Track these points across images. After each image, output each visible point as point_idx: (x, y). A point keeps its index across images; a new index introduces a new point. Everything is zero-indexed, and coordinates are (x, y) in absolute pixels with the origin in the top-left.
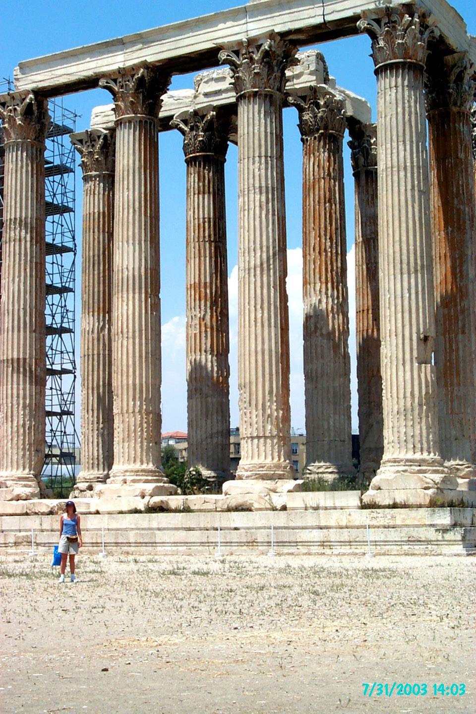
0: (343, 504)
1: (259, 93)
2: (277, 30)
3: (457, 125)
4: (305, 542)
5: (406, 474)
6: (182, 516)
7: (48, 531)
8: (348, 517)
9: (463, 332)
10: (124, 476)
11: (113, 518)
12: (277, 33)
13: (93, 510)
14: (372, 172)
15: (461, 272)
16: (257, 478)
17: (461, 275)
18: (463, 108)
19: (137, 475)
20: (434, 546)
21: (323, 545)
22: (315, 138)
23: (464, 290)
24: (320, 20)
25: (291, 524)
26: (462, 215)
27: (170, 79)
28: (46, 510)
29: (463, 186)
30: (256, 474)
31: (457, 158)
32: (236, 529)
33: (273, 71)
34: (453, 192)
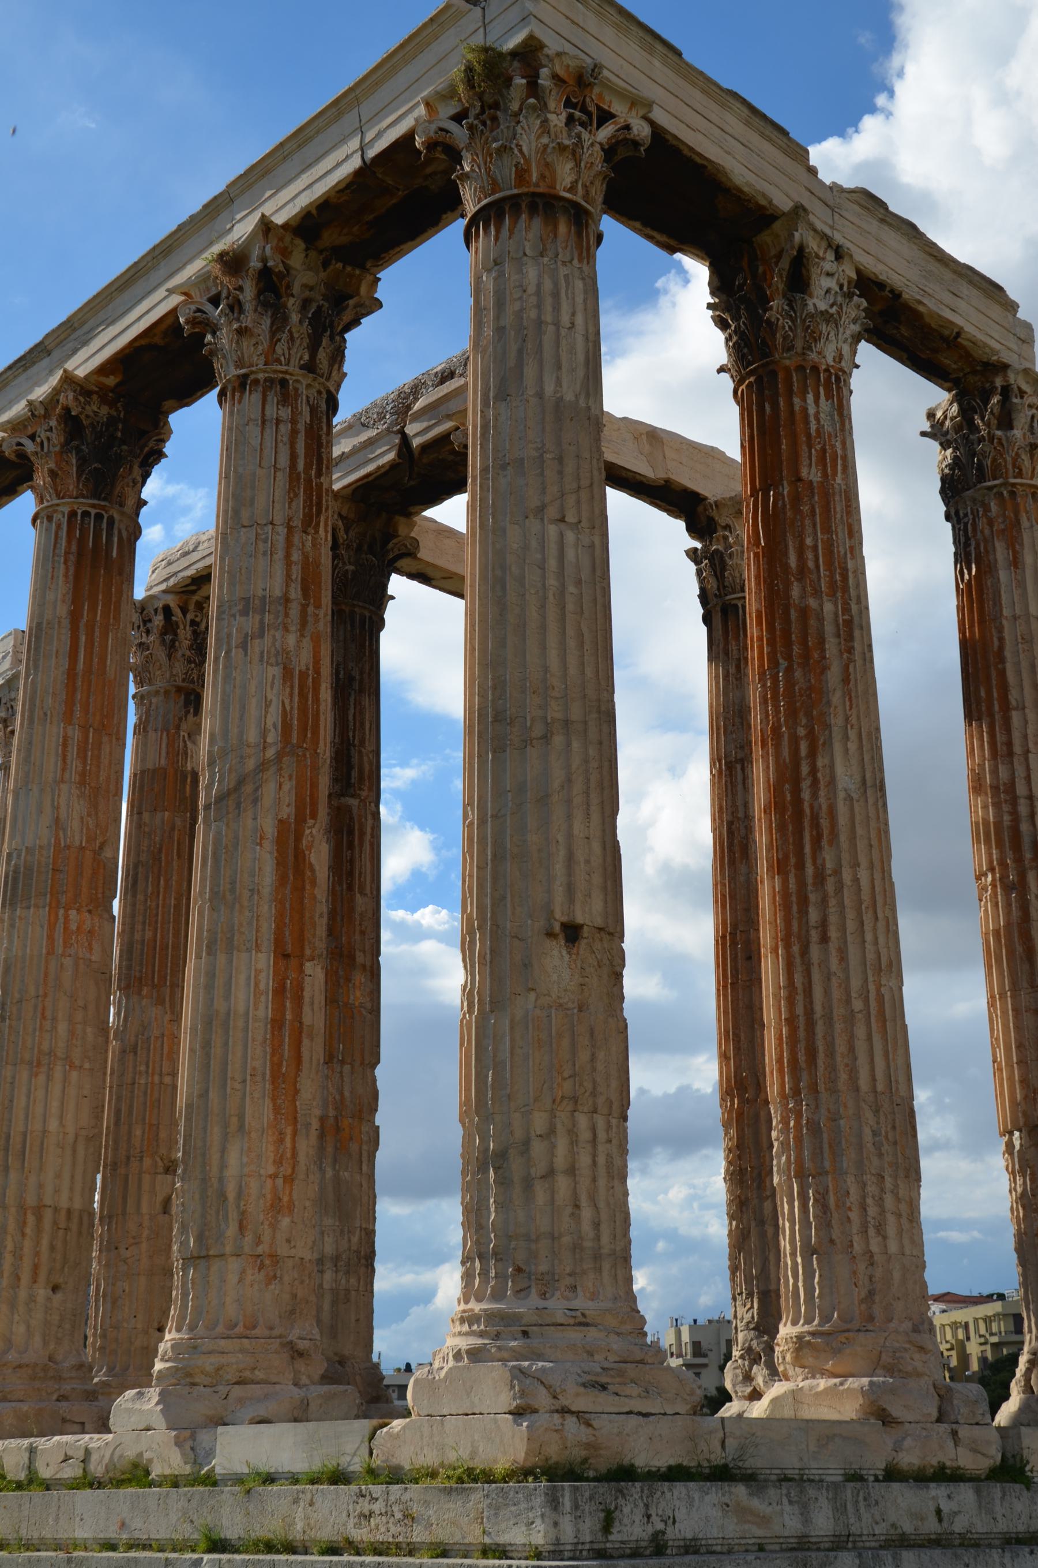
1: (252, 377)
2: (279, 219)
3: (796, 401)
9: (824, 939)
12: (285, 226)
14: (736, 606)
15: (814, 771)
17: (815, 782)
18: (813, 356)
23: (824, 823)
24: (356, 163)
26: (812, 622)
27: (167, 423)
29: (815, 548)
31: (800, 479)
33: (285, 319)
34: (786, 566)
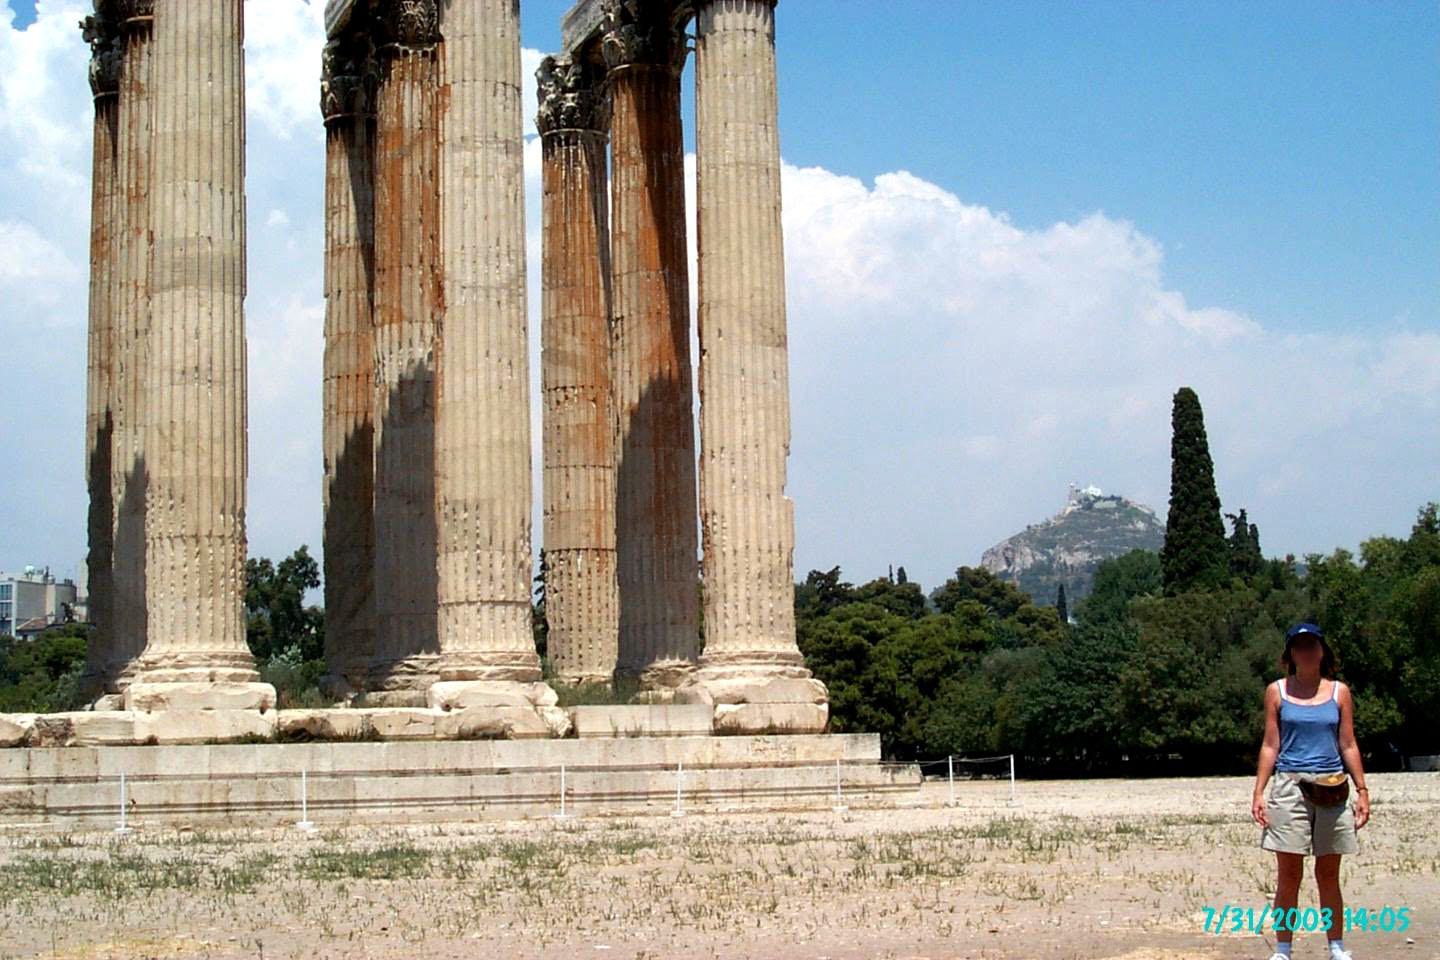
0: (684, 728)
4: (664, 793)
5: (785, 678)
6: (388, 747)
7: (46, 780)
8: (716, 749)
10: (209, 666)
11: (224, 752)
13: (141, 734)
16: (507, 679)
19: (235, 666)
20: (877, 795)
21: (694, 798)
22: (425, 54)
25: (613, 762)
28: (12, 737)
30: (509, 671)
32: (503, 771)
